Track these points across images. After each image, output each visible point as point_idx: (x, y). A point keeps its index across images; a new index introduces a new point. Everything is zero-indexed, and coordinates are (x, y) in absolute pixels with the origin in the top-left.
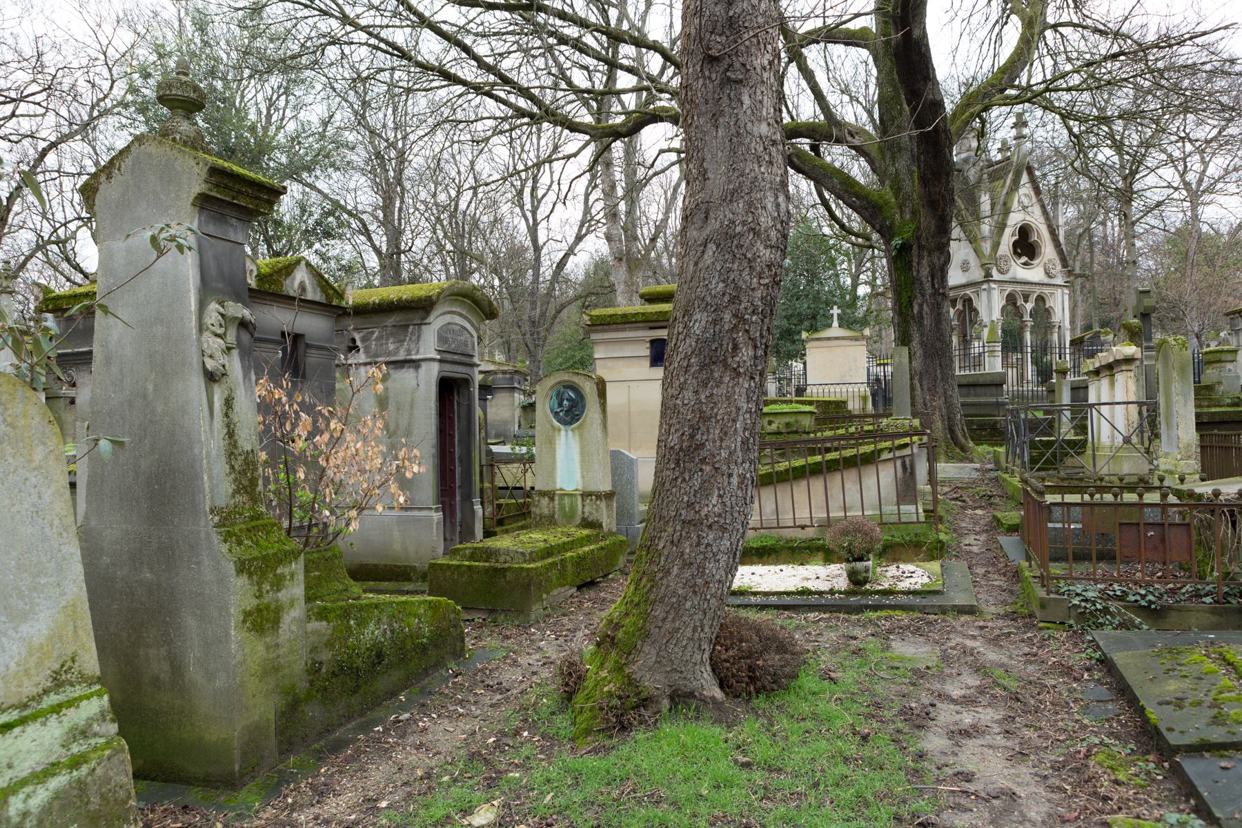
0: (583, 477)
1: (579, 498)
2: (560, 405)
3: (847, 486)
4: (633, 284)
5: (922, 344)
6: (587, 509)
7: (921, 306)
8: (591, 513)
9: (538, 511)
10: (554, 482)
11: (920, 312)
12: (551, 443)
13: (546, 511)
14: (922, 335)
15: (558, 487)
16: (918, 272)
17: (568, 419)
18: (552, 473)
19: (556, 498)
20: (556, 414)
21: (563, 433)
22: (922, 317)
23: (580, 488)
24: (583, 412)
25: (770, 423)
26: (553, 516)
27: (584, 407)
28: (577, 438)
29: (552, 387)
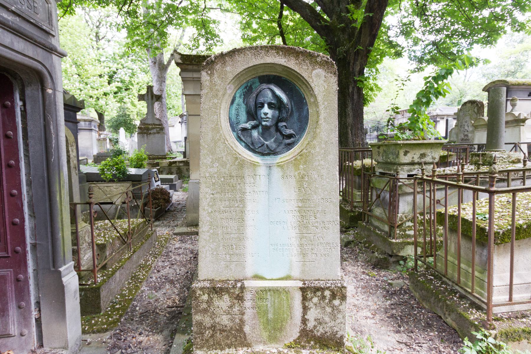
0: (304, 255)
1: (298, 297)
2: (252, 115)
3: (422, 205)
5: (352, 109)
6: (312, 315)
7: (353, 88)
8: (319, 322)
9: (207, 321)
10: (241, 264)
11: (353, 92)
12: (233, 184)
13: (225, 320)
14: (353, 104)
15: (249, 272)
16: (353, 69)
17: (270, 143)
18: (235, 247)
19: (248, 296)
20: (243, 134)
21: (262, 171)
22: (353, 95)
23: (296, 273)
24: (302, 130)
25: (406, 153)
26: (240, 330)
28: (293, 182)
29: (238, 77)
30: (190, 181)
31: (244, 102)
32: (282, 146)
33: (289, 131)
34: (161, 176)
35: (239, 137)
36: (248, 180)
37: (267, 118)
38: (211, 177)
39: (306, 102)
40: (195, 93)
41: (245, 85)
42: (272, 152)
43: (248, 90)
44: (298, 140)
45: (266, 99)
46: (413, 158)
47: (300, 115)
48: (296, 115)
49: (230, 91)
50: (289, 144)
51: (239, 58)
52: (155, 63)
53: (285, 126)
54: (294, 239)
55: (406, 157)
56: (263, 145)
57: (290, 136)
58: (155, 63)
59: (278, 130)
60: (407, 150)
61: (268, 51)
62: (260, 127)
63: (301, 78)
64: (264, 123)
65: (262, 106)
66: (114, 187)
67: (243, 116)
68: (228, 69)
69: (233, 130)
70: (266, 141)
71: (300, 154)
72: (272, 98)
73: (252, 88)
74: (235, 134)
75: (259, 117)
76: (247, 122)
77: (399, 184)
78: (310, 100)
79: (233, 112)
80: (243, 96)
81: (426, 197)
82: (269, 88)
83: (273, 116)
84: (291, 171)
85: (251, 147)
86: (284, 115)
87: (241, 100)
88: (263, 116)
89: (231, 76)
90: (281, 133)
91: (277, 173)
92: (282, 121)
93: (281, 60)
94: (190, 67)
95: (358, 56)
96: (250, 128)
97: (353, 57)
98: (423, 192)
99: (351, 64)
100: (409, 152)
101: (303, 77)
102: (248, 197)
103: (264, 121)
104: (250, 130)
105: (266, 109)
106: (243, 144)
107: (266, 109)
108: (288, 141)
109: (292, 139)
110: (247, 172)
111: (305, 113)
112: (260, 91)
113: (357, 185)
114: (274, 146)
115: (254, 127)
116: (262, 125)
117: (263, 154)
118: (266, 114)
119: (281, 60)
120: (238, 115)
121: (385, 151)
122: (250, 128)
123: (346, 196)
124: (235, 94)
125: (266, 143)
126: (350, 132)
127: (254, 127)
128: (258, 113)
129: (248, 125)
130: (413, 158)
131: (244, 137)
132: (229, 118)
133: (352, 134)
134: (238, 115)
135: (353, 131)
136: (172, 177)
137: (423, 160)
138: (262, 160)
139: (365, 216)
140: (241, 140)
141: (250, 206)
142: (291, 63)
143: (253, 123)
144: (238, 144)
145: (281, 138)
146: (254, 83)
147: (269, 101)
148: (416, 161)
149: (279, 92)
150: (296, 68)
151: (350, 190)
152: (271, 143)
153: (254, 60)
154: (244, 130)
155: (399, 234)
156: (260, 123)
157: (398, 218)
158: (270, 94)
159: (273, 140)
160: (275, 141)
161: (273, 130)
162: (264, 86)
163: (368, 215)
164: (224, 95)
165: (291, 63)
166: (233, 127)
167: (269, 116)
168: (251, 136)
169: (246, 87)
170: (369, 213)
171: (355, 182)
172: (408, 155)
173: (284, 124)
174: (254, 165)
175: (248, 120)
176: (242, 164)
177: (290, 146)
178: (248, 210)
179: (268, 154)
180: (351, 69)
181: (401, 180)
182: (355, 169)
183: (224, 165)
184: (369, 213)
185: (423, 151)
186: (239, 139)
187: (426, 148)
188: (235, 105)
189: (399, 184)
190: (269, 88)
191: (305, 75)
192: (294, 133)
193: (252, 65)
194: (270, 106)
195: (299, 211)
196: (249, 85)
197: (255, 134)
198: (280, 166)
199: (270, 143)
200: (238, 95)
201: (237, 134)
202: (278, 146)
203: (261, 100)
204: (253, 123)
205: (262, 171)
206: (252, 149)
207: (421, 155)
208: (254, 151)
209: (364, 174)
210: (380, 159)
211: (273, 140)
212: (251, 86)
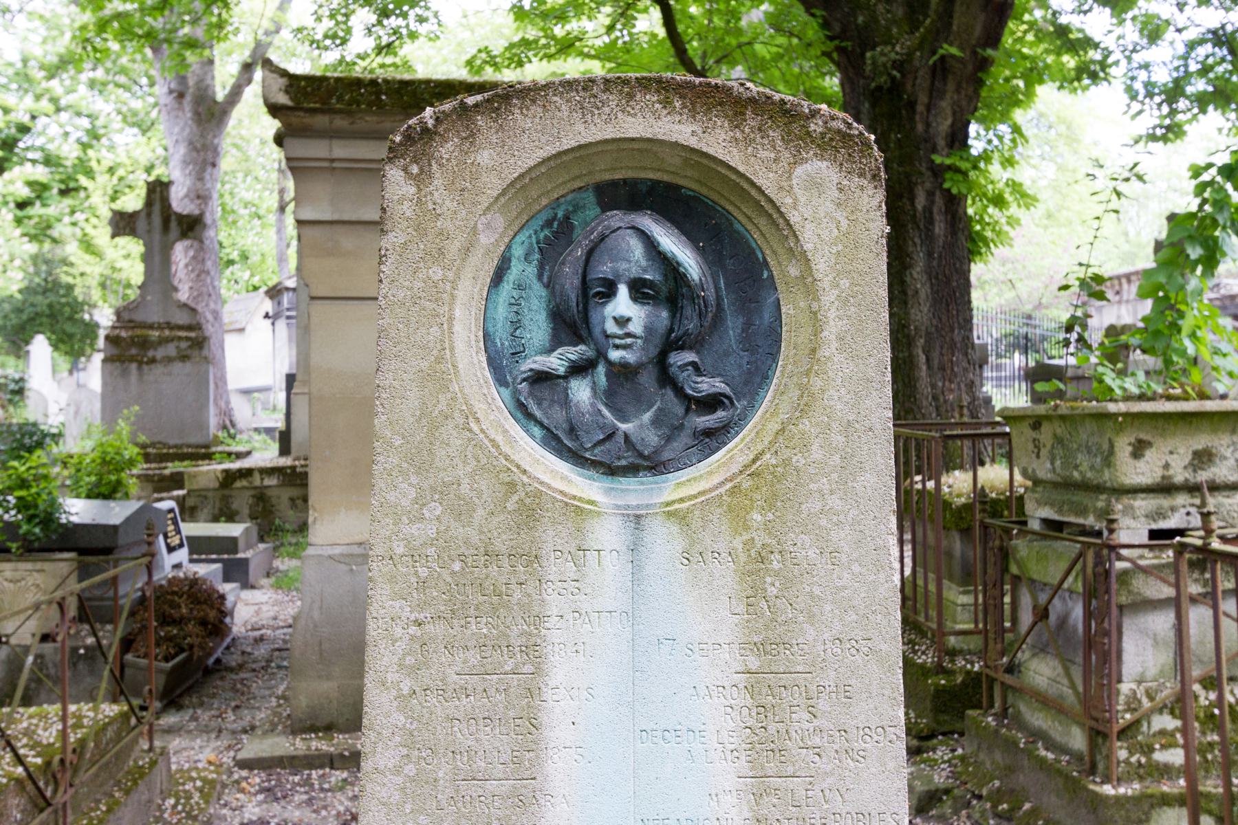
2: (571, 323)
3: (1211, 646)
4: (205, 147)
5: (930, 273)
7: (930, 194)
11: (928, 210)
12: (496, 589)
14: (930, 255)
16: (928, 125)
17: (638, 427)
20: (536, 394)
22: (930, 221)
24: (755, 379)
25: (1139, 450)
27: (763, 347)
28: (724, 575)
30: (310, 551)
31: (540, 277)
32: (684, 439)
33: (708, 385)
34: (190, 529)
35: (522, 407)
36: (554, 567)
37: (629, 335)
38: (414, 556)
39: (771, 277)
40: (336, 217)
41: (544, 217)
42: (650, 464)
43: (556, 234)
44: (743, 419)
45: (623, 266)
46: (1167, 466)
47: (748, 324)
48: (733, 325)
49: (491, 238)
50: (709, 433)
51: (523, 119)
52: (181, 96)
53: (693, 364)
54: (730, 799)
55: (1141, 465)
56: (610, 437)
57: (712, 403)
58: (181, 96)
59: (666, 379)
60: (1143, 436)
61: (631, 96)
62: (601, 369)
63: (753, 192)
64: (615, 355)
65: (609, 290)
66: (8, 574)
67: (538, 328)
68: (485, 157)
69: (501, 380)
70: (624, 419)
71: (752, 470)
72: (644, 263)
73: (571, 228)
74: (506, 393)
75: (597, 331)
76: (550, 351)
77: (1120, 565)
78: (784, 270)
79: (502, 312)
80: (537, 256)
81: (1223, 619)
82: (633, 228)
83: (649, 329)
84: (719, 535)
85: (567, 444)
86: (691, 326)
87: (532, 270)
88: (611, 327)
89: (493, 185)
90: (679, 391)
91: (663, 541)
92: (682, 348)
93: (677, 128)
94: (321, 121)
95: (944, 79)
96: (562, 371)
97: (926, 84)
98: (1211, 598)
99: (920, 108)
100: (1149, 444)
101: (759, 189)
102: (556, 634)
103: (617, 347)
104: (565, 377)
105: (622, 304)
106: (537, 431)
107: (622, 304)
108: (706, 421)
109: (721, 414)
110: (551, 537)
111: (767, 316)
112: (603, 238)
113: (957, 568)
114: (652, 438)
115: (579, 369)
116: (609, 363)
117: (611, 471)
118: (622, 321)
119: (677, 128)
120: (516, 324)
121: (1059, 440)
122: (562, 371)
123: (916, 612)
124: (509, 247)
125: (623, 427)
126: (923, 358)
127: (579, 369)
128: (594, 317)
129: (556, 362)
130: (1167, 466)
131: (539, 404)
132: (486, 336)
133: (929, 367)
134: (516, 324)
135: (935, 355)
136: (234, 530)
137: (1203, 476)
138: (608, 491)
139: (991, 689)
140: (529, 416)
141: (561, 671)
142: (716, 140)
143: (574, 353)
144: (516, 430)
145: (680, 410)
146: (577, 208)
147: (635, 272)
148: (1179, 476)
149: (671, 243)
150: (735, 158)
151: (932, 587)
152: (641, 426)
153: (581, 127)
154: (540, 378)
155: (1127, 762)
156: (601, 354)
157: (1122, 699)
158: (637, 250)
159: (647, 417)
160: (656, 422)
161: (647, 379)
162: (617, 218)
163: (1006, 688)
164: (467, 250)
165: (716, 140)
166: (499, 366)
167: (636, 327)
168: (566, 402)
169: (548, 224)
170: (1008, 679)
171: (949, 554)
172: (1149, 454)
173: (690, 356)
174: (578, 511)
175: (556, 342)
176: (530, 507)
177: (712, 439)
178: (552, 684)
179: (632, 470)
180: (920, 127)
181: (1124, 552)
182: (947, 505)
183: (462, 511)
184: (1008, 679)
185: (1201, 441)
186: (523, 412)
187: (1214, 431)
188: (507, 288)
189: (1120, 565)
190: (633, 228)
191: (766, 180)
192: (727, 390)
193: (573, 144)
194: (639, 291)
195: (750, 689)
196: (560, 214)
197: (581, 391)
198: (675, 515)
199: (638, 427)
200: (518, 251)
201: (515, 394)
202: (669, 439)
203: (604, 269)
204: (574, 353)
205: (608, 534)
206: (570, 450)
207: (1197, 455)
208: (576, 457)
209: (985, 527)
210: (1044, 470)
211: (647, 417)
212: (567, 218)
